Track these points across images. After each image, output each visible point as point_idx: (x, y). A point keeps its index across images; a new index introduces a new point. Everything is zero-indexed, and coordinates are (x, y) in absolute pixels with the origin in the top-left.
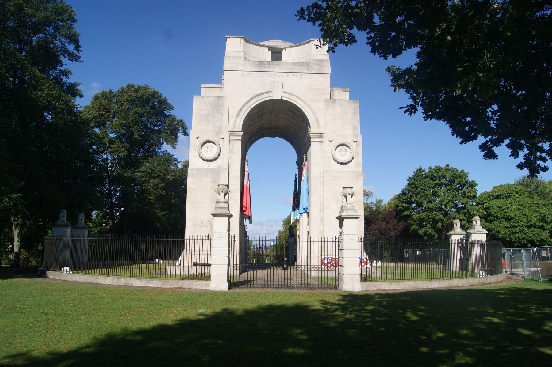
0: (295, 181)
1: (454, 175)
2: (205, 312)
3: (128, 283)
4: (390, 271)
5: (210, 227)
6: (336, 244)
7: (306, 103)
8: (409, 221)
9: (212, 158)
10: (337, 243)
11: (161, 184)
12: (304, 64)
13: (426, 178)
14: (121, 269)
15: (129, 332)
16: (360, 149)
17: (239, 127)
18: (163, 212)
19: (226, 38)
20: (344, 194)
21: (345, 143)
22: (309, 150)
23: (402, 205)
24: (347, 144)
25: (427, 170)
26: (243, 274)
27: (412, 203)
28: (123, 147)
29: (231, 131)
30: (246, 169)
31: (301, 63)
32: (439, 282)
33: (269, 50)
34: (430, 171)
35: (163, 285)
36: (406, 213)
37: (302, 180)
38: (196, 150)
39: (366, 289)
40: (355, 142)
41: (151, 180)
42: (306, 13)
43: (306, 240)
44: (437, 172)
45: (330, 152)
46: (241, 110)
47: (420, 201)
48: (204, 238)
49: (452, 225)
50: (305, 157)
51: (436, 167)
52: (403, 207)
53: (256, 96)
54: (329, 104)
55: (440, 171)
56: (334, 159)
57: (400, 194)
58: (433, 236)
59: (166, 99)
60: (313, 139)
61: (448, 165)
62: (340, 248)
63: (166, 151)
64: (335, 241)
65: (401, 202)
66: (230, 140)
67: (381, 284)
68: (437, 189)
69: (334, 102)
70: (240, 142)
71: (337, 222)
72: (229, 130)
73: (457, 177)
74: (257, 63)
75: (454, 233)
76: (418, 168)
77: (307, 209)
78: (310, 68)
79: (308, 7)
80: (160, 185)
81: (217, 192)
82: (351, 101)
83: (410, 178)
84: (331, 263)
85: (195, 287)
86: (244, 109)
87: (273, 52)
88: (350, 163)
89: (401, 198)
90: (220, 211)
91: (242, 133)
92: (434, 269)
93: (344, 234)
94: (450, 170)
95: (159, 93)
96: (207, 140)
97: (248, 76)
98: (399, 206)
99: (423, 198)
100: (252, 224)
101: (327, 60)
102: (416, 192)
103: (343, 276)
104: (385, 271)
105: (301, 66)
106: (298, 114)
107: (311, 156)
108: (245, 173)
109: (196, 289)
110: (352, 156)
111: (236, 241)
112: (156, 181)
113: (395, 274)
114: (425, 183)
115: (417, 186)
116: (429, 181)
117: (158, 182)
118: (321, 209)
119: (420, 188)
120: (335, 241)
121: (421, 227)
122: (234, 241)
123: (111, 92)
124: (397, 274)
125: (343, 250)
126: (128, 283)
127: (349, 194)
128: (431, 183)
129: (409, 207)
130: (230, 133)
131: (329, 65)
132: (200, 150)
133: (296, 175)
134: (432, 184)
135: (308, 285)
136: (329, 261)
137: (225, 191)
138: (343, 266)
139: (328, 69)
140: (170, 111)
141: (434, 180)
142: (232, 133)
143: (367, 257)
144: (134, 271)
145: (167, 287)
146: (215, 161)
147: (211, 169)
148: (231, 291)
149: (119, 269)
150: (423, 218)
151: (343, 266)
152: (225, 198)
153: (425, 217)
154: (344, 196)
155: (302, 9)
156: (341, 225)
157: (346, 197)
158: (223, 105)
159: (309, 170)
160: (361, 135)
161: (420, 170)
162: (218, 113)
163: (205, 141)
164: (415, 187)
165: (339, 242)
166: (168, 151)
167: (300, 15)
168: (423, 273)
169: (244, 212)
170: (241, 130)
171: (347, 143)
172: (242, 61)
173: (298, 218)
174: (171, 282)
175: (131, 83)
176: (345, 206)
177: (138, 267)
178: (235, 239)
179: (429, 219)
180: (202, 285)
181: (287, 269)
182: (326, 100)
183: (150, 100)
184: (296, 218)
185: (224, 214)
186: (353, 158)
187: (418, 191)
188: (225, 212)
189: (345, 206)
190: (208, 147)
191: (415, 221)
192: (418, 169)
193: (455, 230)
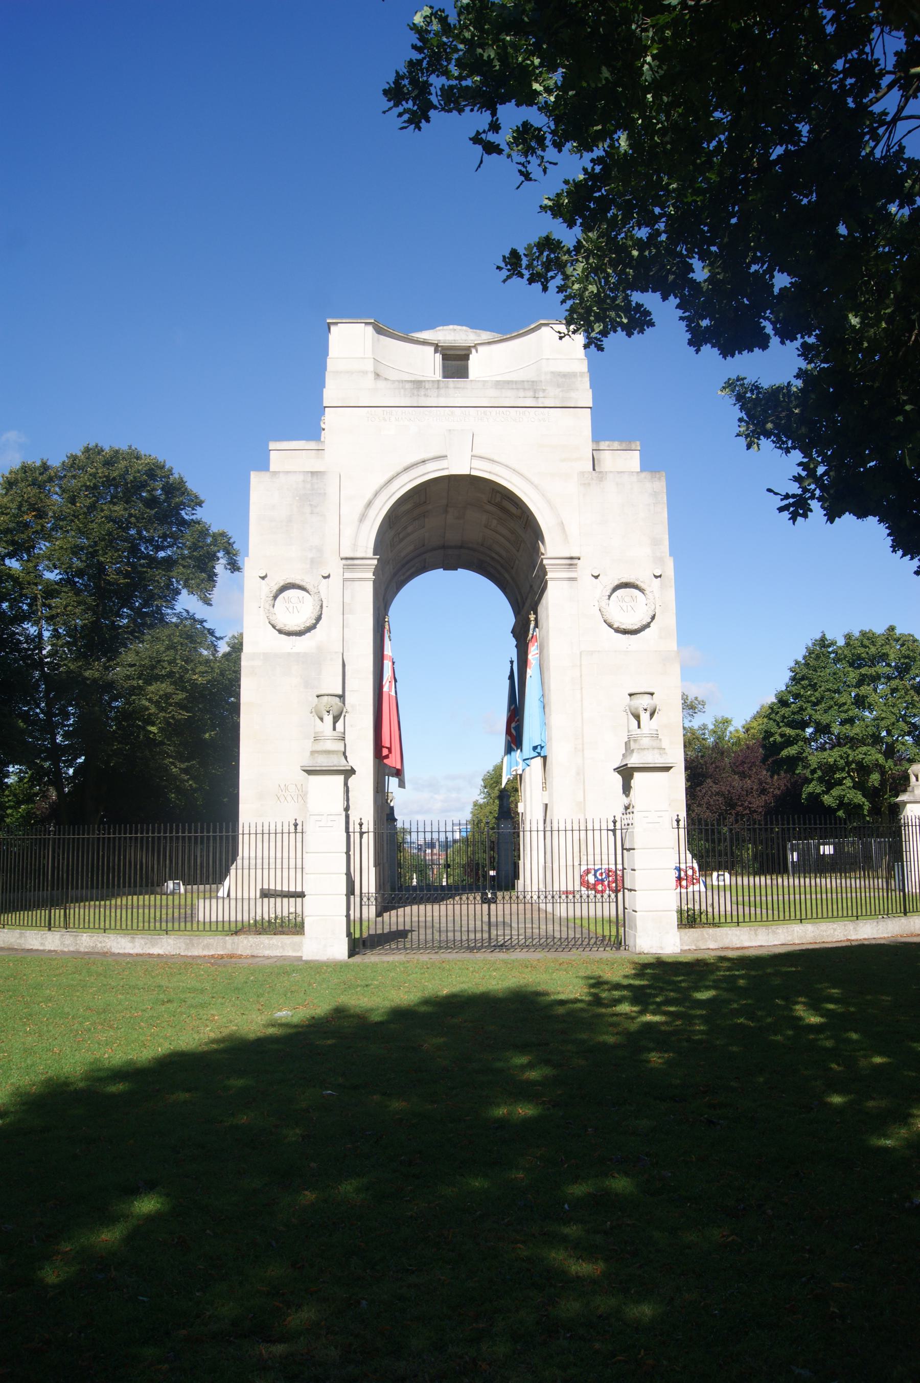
0: (511, 677)
1: (908, 652)
2: (292, 1016)
3: (99, 945)
4: (752, 899)
5: (300, 798)
6: (615, 835)
8: (797, 772)
9: (301, 627)
10: (618, 833)
11: (178, 694)
12: (526, 383)
13: (837, 660)
14: (82, 911)
15: (101, 1074)
16: (671, 594)
17: (367, 547)
18: (183, 762)
19: (329, 325)
20: (633, 711)
22: (543, 601)
23: (779, 731)
25: (841, 642)
26: (386, 915)
27: (803, 725)
28: (80, 603)
29: (346, 559)
30: (386, 653)
31: (516, 382)
32: (875, 924)
33: (436, 351)
34: (848, 644)
35: (187, 949)
36: (791, 751)
37: (528, 676)
38: (262, 609)
39: (695, 948)
40: (656, 577)
41: (151, 684)
42: (525, 262)
43: (541, 828)
44: (866, 647)
46: (369, 504)
47: (825, 719)
48: (286, 830)
49: (907, 778)
50: (532, 617)
51: (863, 634)
52: (782, 735)
53: (407, 469)
54: (589, 484)
55: (873, 644)
56: (605, 621)
57: (773, 703)
58: (860, 807)
59: (182, 482)
61: (892, 629)
62: (627, 846)
63: (187, 611)
64: (613, 828)
65: (778, 725)
66: (345, 580)
67: (729, 932)
68: (865, 690)
69: (602, 477)
70: (371, 583)
71: (618, 779)
72: (343, 555)
73: (915, 658)
74: (408, 386)
75: (911, 799)
76: (818, 636)
77: (542, 747)
78: (541, 394)
79: (529, 248)
80: (174, 696)
81: (314, 713)
82: (644, 475)
83: (797, 663)
84: (606, 883)
85: (267, 953)
86: (378, 503)
87: (445, 358)
88: (647, 630)
89: (778, 713)
90: (323, 762)
91: (375, 562)
92: (863, 890)
93: (635, 810)
94: (897, 640)
95: (164, 466)
97: (385, 420)
98: (772, 734)
99: (833, 712)
100: (404, 787)
101: (582, 374)
102: (813, 699)
103: (635, 916)
104: (740, 899)
105: (517, 389)
106: (513, 509)
107: (547, 616)
109: (268, 958)
110: (652, 614)
111: (365, 836)
112: (165, 687)
113: (764, 906)
114: (834, 674)
115: (816, 683)
116: (846, 670)
117: (169, 690)
118: (575, 748)
119: (823, 688)
120: (613, 828)
121: (830, 786)
122: (362, 834)
123: (45, 467)
124: (770, 906)
125: (634, 849)
126: (99, 945)
127: (646, 710)
128: (852, 675)
129: (798, 735)
130: (344, 562)
133: (512, 662)
134: (853, 676)
135: (549, 941)
136: (600, 878)
137: (335, 711)
138: (635, 891)
139: (586, 398)
140: (194, 512)
141: (859, 667)
142: (350, 562)
143: (696, 866)
144: (113, 914)
145: (196, 953)
147: (298, 654)
148: (357, 959)
149: (77, 910)
150: (834, 764)
151: (635, 891)
152: (334, 729)
153: (838, 759)
154: (632, 714)
155: (514, 254)
156: (627, 789)
157: (637, 717)
158: (325, 494)
159: (545, 651)
160: (672, 559)
161: (823, 642)
162: (312, 513)
163: (282, 584)
164: (810, 685)
165: (624, 831)
166: (192, 612)
167: (509, 267)
168: (835, 901)
169: (386, 761)
170: (370, 553)
173: (520, 772)
174: (206, 942)
175: (94, 445)
176: (635, 741)
177: (124, 902)
178: (363, 830)
179: (848, 764)
180: (283, 947)
181: (494, 900)
182: (583, 473)
183: (143, 485)
184: (516, 770)
185: (335, 768)
186: (653, 618)
187: (817, 694)
188: (336, 763)
189: (635, 741)
190: (289, 600)
191: (813, 772)
192: (816, 641)
193: (913, 791)
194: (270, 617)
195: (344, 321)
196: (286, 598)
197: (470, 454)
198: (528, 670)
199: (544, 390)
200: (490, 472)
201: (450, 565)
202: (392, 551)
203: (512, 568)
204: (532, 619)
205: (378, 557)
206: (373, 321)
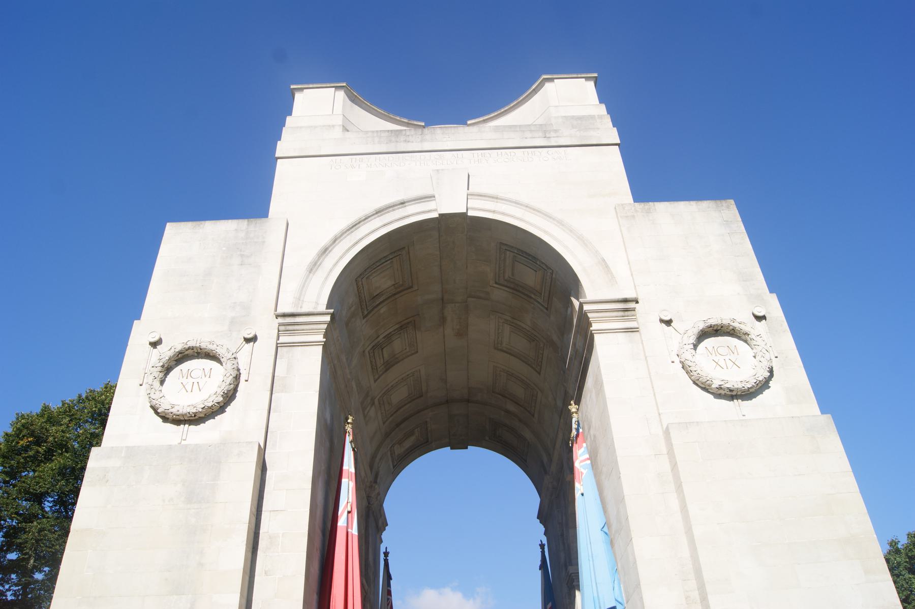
0: (543, 566)
7: (554, 219)
16: (786, 344)
21: (725, 322)
24: (736, 325)
29: (284, 315)
30: (345, 467)
45: (677, 360)
46: (325, 251)
53: (379, 212)
60: (597, 322)
70: (318, 351)
72: (280, 310)
78: (553, 134)
88: (766, 392)
91: (328, 318)
96: (191, 344)
101: (601, 117)
106: (530, 278)
108: (344, 481)
110: (766, 364)
118: (687, 598)
130: (281, 320)
131: (611, 124)
132: (157, 384)
133: (542, 546)
146: (210, 422)
147: (186, 446)
158: (264, 242)
160: (774, 295)
163: (179, 348)
170: (322, 308)
171: (734, 320)
172: (338, 132)
190: (189, 373)
194: (152, 396)
195: (311, 86)
196: (185, 371)
197: (465, 191)
198: (577, 485)
199: (556, 131)
200: (494, 212)
201: (459, 443)
202: (375, 381)
203: (533, 416)
204: (574, 410)
205: (332, 311)
206: (345, 84)
